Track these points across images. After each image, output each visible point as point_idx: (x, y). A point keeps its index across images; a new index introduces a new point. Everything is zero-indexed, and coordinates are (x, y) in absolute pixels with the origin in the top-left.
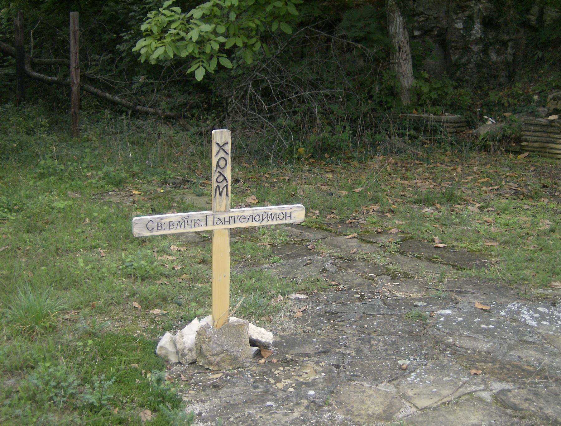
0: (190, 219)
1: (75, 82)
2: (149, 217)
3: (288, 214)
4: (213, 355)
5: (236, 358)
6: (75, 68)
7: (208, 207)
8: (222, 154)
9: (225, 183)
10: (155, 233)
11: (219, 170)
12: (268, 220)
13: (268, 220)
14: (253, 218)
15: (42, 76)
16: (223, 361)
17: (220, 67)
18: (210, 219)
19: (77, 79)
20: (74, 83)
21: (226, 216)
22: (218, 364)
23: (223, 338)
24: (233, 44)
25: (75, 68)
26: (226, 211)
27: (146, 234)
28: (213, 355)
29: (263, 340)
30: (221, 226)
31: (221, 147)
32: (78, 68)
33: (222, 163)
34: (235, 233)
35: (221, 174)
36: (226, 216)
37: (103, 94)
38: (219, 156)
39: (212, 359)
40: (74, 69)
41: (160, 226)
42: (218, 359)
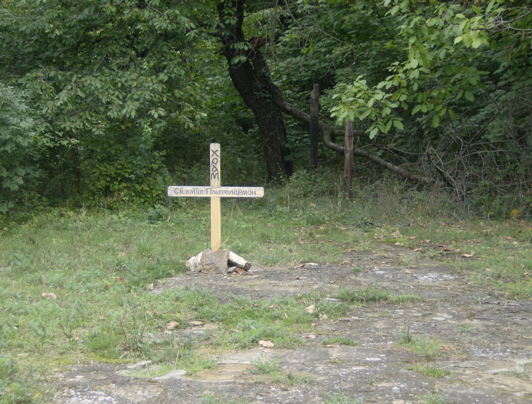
0: (198, 190)
1: (348, 149)
2: (176, 187)
3: (254, 192)
4: (206, 265)
5: (217, 268)
6: (349, 136)
7: (209, 184)
8: (215, 156)
9: (217, 172)
10: (179, 195)
11: (213, 164)
12: (242, 194)
13: (242, 194)
14: (233, 193)
15: (336, 145)
16: (211, 269)
17: (393, 129)
18: (209, 191)
19: (350, 146)
20: (347, 150)
21: (218, 189)
22: (208, 270)
23: (214, 257)
24: (418, 110)
25: (349, 136)
26: (217, 187)
27: (174, 195)
28: (206, 265)
29: (239, 263)
30: (215, 195)
31: (214, 152)
32: (351, 136)
33: (215, 161)
34: (223, 200)
35: (215, 167)
36: (218, 189)
37: (385, 163)
38: (213, 157)
39: (205, 267)
40: (347, 138)
41: (181, 192)
42: (208, 267)
